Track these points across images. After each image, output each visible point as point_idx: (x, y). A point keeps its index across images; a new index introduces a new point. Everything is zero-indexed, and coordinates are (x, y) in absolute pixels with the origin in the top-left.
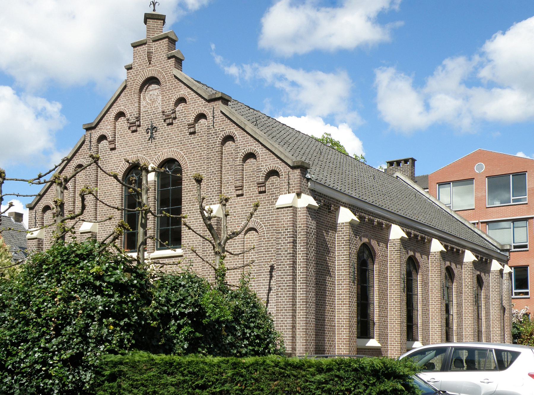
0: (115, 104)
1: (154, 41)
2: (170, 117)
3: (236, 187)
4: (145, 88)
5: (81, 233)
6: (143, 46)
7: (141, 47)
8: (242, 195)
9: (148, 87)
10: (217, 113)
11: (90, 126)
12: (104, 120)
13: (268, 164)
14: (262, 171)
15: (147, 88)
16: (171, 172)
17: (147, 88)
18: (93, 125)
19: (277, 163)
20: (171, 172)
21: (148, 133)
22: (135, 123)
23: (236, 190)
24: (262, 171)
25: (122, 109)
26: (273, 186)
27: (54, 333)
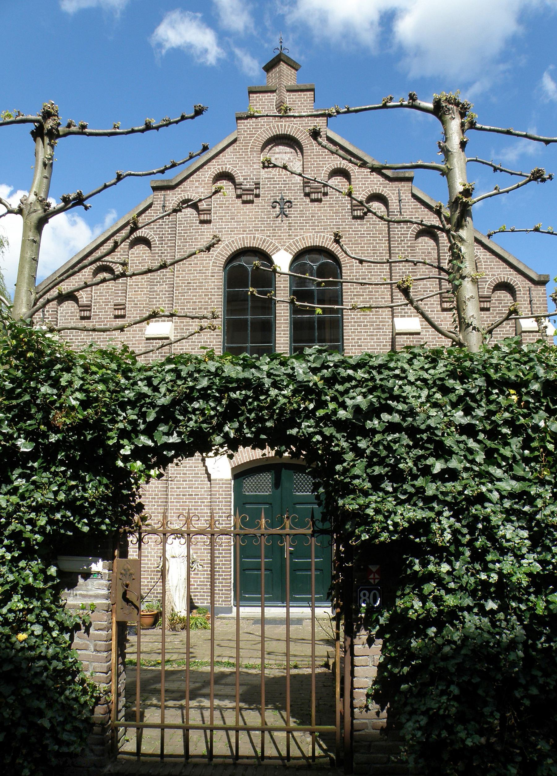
0: (214, 161)
1: (288, 91)
2: (319, 190)
3: (115, 305)
4: (270, 146)
5: (148, 339)
6: (269, 94)
7: (266, 95)
8: (488, 309)
9: (272, 147)
10: (407, 197)
11: (165, 184)
12: (191, 178)
13: (496, 273)
14: (487, 281)
15: (271, 149)
16: (320, 267)
17: (271, 149)
18: (173, 183)
19: (510, 275)
20: (320, 267)
21: (274, 207)
22: (253, 191)
23: (115, 309)
24: (487, 281)
25: (229, 168)
26: (501, 303)
27: (530, 543)
